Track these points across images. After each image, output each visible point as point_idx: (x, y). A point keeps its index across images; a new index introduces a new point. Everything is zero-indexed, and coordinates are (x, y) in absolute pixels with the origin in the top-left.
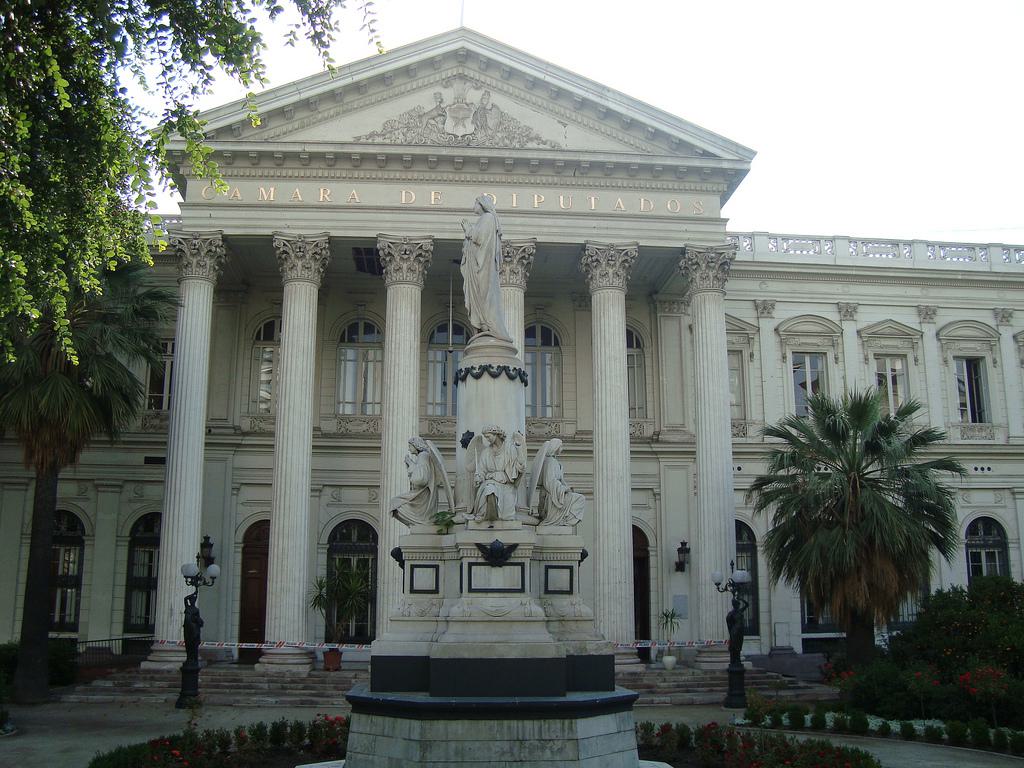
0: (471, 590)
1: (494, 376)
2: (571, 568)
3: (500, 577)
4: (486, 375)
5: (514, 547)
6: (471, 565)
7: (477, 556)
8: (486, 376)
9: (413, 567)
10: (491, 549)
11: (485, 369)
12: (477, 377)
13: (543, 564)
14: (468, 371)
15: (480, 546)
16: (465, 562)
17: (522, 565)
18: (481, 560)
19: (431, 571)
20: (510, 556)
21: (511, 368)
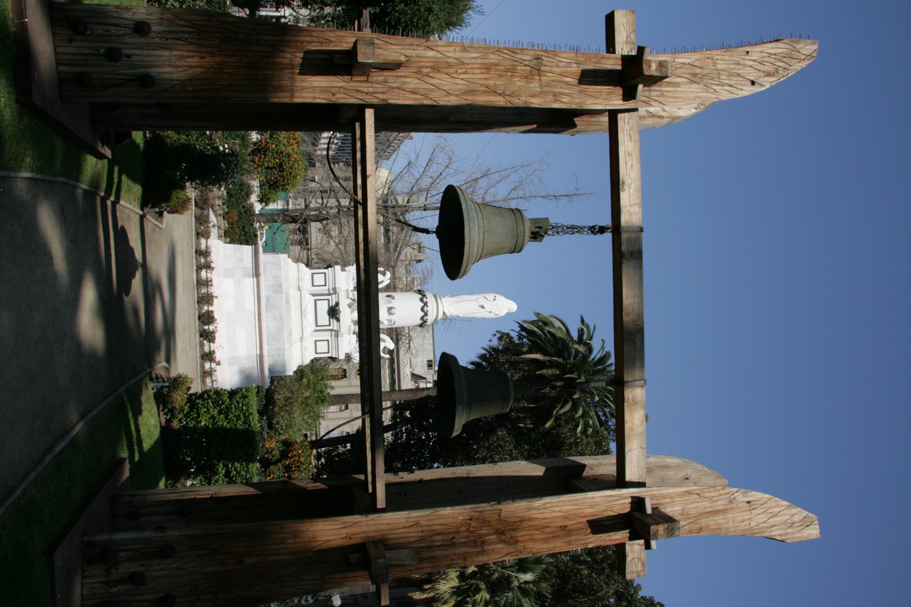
0: (316, 301)
1: (422, 309)
2: (328, 352)
3: (324, 318)
4: (422, 304)
5: (338, 320)
6: (328, 300)
7: (333, 303)
8: (422, 304)
9: (325, 273)
10: (336, 310)
11: (426, 304)
12: (421, 300)
13: (329, 338)
14: (424, 296)
15: (337, 304)
16: (329, 297)
17: (330, 325)
18: (331, 305)
19: (324, 284)
20: (333, 318)
21: (427, 317)
